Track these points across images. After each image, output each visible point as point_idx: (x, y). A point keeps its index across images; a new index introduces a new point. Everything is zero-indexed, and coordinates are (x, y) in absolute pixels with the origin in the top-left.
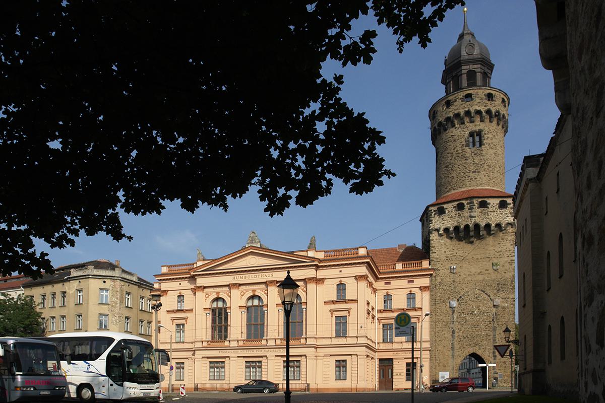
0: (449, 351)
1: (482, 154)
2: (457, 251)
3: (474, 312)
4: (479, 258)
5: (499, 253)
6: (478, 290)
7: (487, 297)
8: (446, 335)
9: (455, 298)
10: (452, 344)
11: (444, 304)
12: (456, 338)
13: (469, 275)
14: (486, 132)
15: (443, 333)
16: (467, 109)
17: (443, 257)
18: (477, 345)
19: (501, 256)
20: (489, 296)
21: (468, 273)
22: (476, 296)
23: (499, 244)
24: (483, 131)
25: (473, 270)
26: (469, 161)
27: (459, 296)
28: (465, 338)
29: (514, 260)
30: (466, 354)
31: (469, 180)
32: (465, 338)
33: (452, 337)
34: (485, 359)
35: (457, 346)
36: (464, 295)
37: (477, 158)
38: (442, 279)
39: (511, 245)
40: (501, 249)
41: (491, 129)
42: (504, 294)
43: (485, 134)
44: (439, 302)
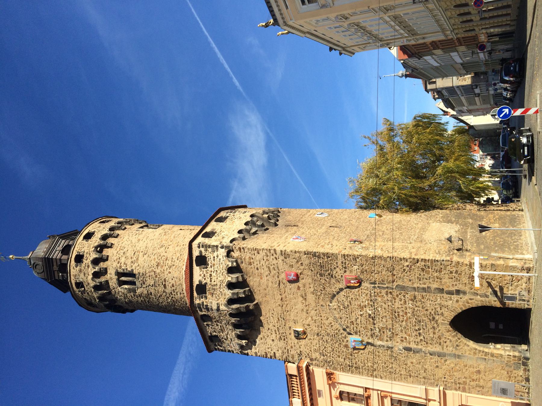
0: (446, 361)
1: (143, 274)
3: (370, 315)
4: (280, 297)
6: (331, 303)
7: (342, 293)
8: (414, 361)
9: (345, 337)
10: (431, 355)
12: (420, 347)
14: (119, 265)
15: (409, 364)
16: (93, 290)
17: (281, 344)
18: (434, 318)
20: (341, 290)
21: (305, 313)
22: (341, 308)
23: (257, 269)
24: (117, 270)
25: (300, 306)
26: (153, 291)
27: (342, 331)
28: (420, 334)
29: (281, 251)
30: (453, 337)
33: (418, 352)
34: (464, 309)
35: (437, 349)
36: (340, 324)
38: (315, 350)
41: (115, 258)
43: (121, 266)
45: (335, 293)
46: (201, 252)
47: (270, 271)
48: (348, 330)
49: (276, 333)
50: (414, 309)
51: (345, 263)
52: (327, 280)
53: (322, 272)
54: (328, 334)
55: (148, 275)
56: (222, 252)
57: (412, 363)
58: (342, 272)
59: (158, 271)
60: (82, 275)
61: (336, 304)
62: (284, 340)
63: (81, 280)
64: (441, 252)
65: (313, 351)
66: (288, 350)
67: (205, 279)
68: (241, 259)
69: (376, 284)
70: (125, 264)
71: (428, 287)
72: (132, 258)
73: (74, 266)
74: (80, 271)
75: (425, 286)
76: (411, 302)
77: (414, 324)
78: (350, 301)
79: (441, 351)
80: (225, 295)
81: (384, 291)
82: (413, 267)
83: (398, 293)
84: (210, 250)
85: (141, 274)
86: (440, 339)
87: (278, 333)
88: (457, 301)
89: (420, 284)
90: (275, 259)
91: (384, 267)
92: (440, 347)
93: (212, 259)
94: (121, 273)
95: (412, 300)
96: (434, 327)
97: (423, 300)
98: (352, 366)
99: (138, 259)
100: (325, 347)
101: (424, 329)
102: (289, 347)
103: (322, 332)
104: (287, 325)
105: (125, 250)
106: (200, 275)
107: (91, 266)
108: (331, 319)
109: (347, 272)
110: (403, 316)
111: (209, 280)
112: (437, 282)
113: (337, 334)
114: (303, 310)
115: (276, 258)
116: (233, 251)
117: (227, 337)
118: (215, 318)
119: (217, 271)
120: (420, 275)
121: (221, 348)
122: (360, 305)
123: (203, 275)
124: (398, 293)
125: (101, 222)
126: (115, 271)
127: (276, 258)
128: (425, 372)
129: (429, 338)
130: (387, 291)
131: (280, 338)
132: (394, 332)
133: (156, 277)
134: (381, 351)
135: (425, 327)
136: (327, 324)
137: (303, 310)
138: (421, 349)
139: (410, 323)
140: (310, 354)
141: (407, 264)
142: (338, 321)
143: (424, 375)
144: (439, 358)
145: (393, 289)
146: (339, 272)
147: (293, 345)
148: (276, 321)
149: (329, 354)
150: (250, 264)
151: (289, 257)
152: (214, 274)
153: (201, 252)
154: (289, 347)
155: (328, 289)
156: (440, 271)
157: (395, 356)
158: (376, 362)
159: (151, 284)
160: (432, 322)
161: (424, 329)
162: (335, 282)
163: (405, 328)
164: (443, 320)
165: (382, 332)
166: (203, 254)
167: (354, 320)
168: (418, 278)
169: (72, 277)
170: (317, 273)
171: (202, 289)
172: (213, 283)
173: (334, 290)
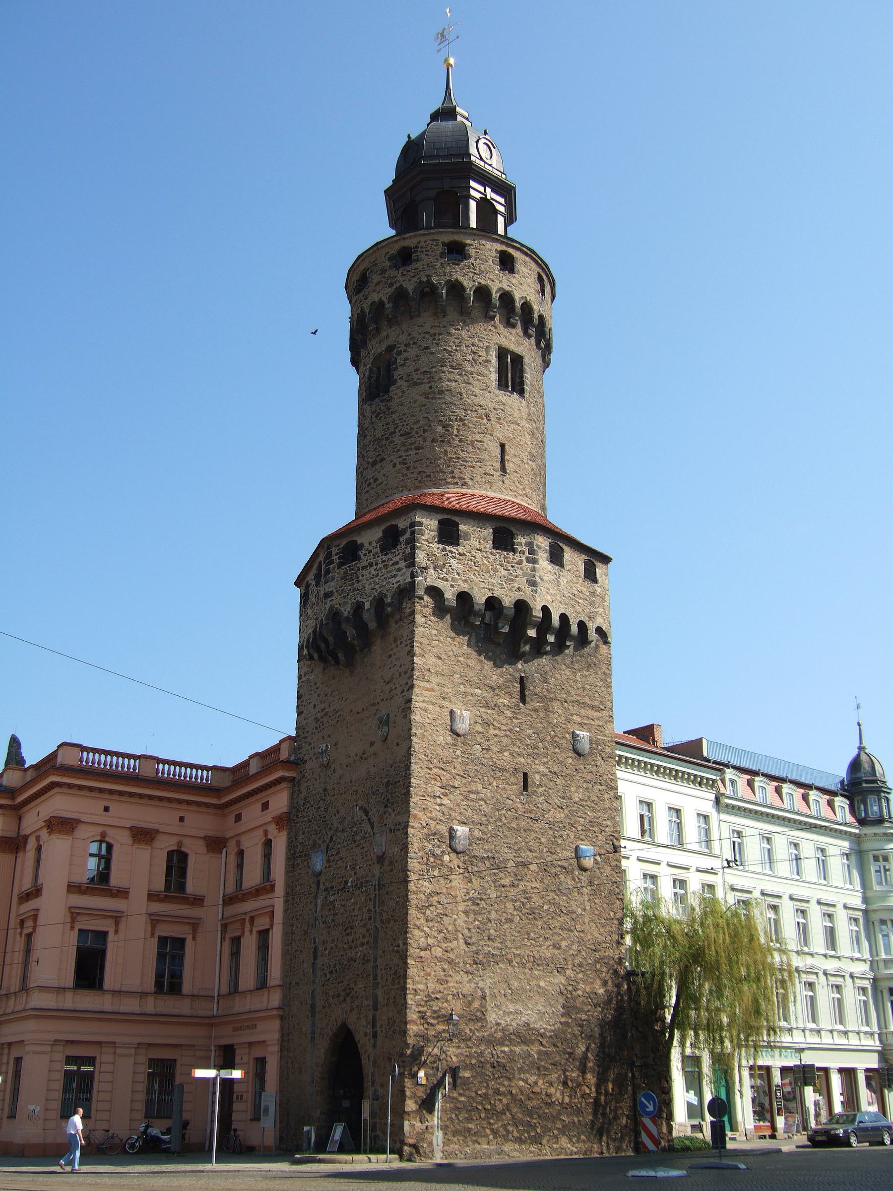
3: (346, 882)
12: (319, 973)
41: (414, 334)
70: (406, 359)
88: (366, 1034)
133: (387, 439)
143: (293, 983)
166: (401, 539)
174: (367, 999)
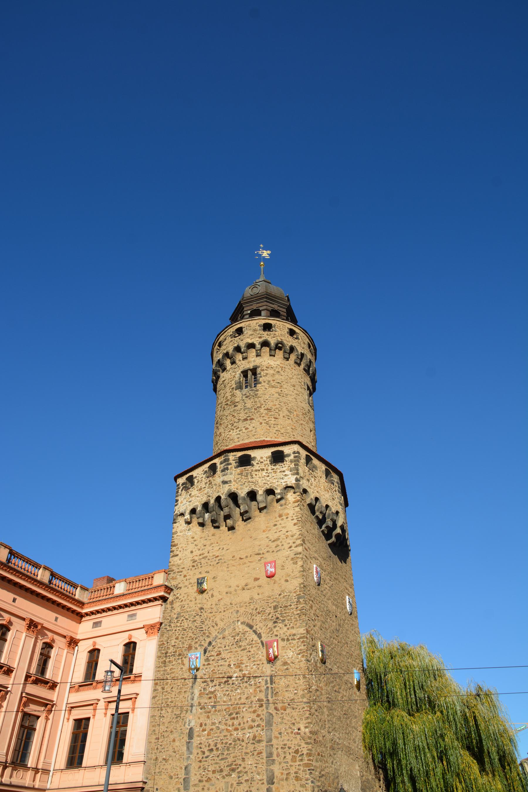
2: (210, 548)
5: (276, 543)
6: (242, 623)
7: (255, 637)
8: (177, 743)
9: (201, 645)
10: (186, 768)
11: (180, 661)
12: (195, 751)
13: (227, 593)
14: (265, 368)
15: (172, 737)
16: (236, 345)
17: (188, 563)
18: (233, 770)
19: (278, 548)
20: (259, 636)
22: (237, 638)
23: (275, 525)
24: (259, 367)
25: (234, 583)
26: (239, 407)
27: (208, 640)
28: (212, 750)
31: (238, 432)
32: (212, 750)
33: (188, 748)
36: (216, 636)
37: (249, 401)
38: (183, 607)
39: (295, 525)
40: (278, 534)
42: (285, 629)
43: (263, 370)
44: (172, 659)
45: (254, 629)
46: (289, 455)
47: (274, 541)
48: (210, 648)
49: (200, 555)
50: (243, 741)
51: (294, 639)
52: (271, 616)
53: (280, 609)
54: (203, 622)
55: (256, 399)
56: (291, 480)
57: (174, 741)
58: (283, 636)
59: (262, 410)
60: (250, 332)
61: (241, 630)
62: (193, 566)
63: (245, 332)
64: (323, 779)
65: (182, 603)
66: (181, 572)
67: (258, 464)
68: (285, 504)
69: (271, 684)
71: (274, 760)
72: (274, 380)
73: (260, 323)
74: (255, 330)
75: (275, 757)
76: (251, 735)
77: (224, 742)
78: (246, 649)
79: (191, 783)
80: (241, 489)
81: (262, 696)
82: (298, 737)
83: (262, 716)
84: (293, 466)
85: (256, 392)
86: (207, 781)
87: (201, 557)
89: (277, 749)
90: (289, 545)
91: (295, 694)
92: (197, 782)
93: (282, 469)
94: (256, 372)
95: (255, 737)
96: (221, 771)
97: (255, 753)
98: (166, 657)
99: (273, 387)
100: (187, 619)
101: (218, 756)
102: (185, 572)
103: (205, 614)
104: (211, 568)
105: (282, 372)
106: (262, 458)
107: (261, 340)
108: (221, 625)
109: (282, 643)
110: (233, 725)
111: (257, 468)
112: (282, 774)
113: (204, 633)
114: (230, 587)
115: (290, 547)
116: (294, 493)
117: (193, 496)
118: (214, 480)
119: (268, 476)
120: (289, 748)
121: (180, 491)
122: (241, 663)
123: (262, 460)
124: (262, 716)
125: (309, 344)
126: (258, 365)
127: (290, 547)
128: (164, 759)
129: (206, 764)
130: (262, 700)
131: (194, 561)
132: (212, 713)
134: (186, 696)
135: (220, 757)
136: (215, 620)
137: (230, 587)
138: (191, 753)
139: (225, 736)
140: (178, 600)
141: (302, 728)
142: (220, 634)
143: (160, 759)
144: (182, 780)
145: (267, 708)
146: (281, 632)
147: (188, 577)
148: (214, 554)
149: (179, 624)
150: (280, 516)
151: (294, 563)
152: (264, 473)
153: (289, 455)
154: (185, 572)
155: (258, 618)
156: (297, 778)
157: (182, 716)
158: (173, 689)
159: (246, 405)
160: (229, 768)
161: (218, 756)
162: (269, 626)
163: (218, 728)
164: (232, 785)
165: (210, 696)
166: (286, 459)
167: (223, 655)
168: (285, 745)
169: (247, 323)
170: (278, 602)
171: (245, 461)
172: (254, 473)
173: (260, 627)
174: (258, 774)
